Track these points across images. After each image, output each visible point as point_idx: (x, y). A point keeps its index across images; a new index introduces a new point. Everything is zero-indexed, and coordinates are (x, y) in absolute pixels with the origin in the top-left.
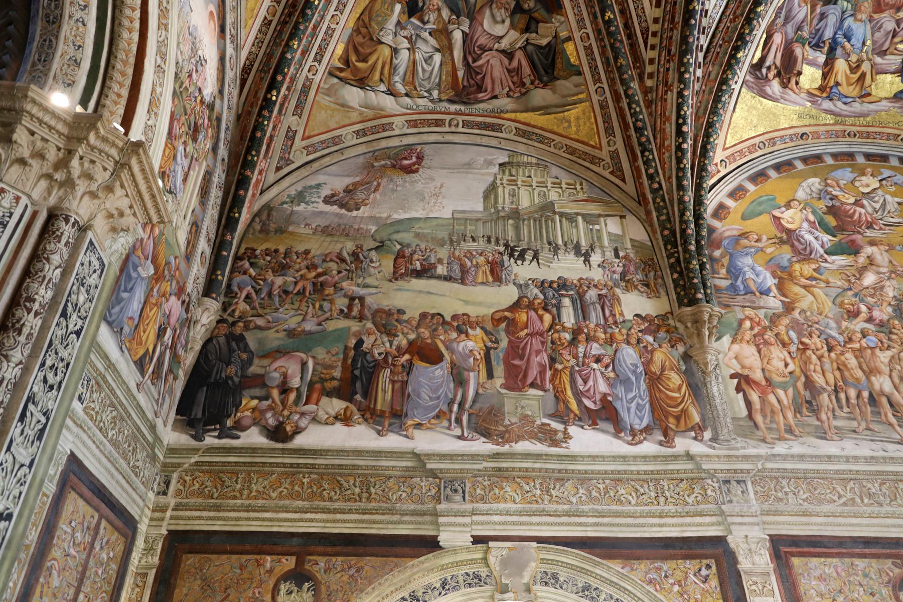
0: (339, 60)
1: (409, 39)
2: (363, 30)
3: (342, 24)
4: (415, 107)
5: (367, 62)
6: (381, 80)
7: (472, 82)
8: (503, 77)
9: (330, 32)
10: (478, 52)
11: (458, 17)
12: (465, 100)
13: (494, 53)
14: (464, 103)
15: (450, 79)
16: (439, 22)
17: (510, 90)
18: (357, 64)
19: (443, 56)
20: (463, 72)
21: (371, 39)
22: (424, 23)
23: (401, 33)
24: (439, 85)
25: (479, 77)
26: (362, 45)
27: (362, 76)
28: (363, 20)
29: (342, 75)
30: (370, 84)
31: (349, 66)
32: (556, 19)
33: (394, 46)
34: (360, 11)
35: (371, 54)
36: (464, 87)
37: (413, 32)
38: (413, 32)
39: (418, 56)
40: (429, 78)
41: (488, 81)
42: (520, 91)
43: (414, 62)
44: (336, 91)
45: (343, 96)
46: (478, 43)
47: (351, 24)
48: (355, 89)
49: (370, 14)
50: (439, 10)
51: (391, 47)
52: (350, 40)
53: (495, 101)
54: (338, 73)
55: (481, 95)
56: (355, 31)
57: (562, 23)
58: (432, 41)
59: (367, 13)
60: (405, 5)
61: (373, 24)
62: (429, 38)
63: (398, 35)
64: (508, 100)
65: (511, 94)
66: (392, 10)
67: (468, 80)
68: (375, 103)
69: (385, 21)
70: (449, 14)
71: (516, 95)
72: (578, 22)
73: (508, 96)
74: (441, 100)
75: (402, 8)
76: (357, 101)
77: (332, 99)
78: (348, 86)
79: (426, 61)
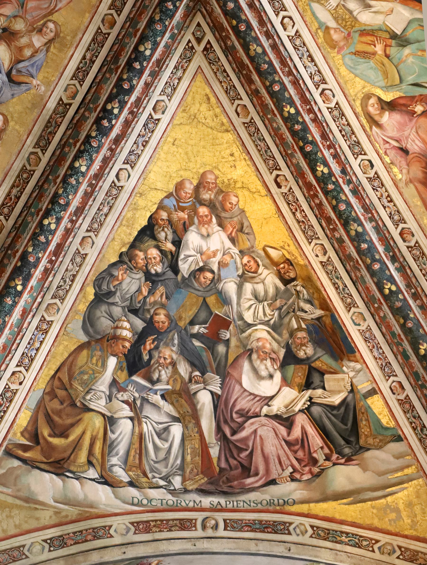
0: (22, 433)
1: (132, 405)
2: (61, 393)
3: (27, 384)
4: (145, 502)
5: (67, 437)
6: (90, 463)
7: (233, 462)
8: (281, 452)
9: (9, 394)
10: (239, 420)
11: (203, 373)
12: (225, 489)
13: (263, 420)
14: (225, 493)
15: (198, 459)
16: (175, 380)
17: (295, 470)
18: (51, 439)
19: (185, 427)
20: (217, 448)
21: (73, 404)
22: (153, 383)
23: (119, 396)
24: (182, 468)
25: (243, 455)
26: (59, 413)
27: (56, 456)
28: (60, 379)
29: (27, 455)
30: (72, 468)
31: (37, 443)
32: (348, 367)
33: (109, 414)
34: (54, 367)
35: (72, 425)
36: (222, 470)
37: (137, 395)
38: (137, 395)
39: (147, 428)
40: (166, 459)
41: (258, 460)
42: (311, 472)
43: (141, 437)
44: (17, 477)
45: (29, 489)
46: (237, 408)
47: (42, 385)
48: (47, 476)
49: (70, 370)
50: (174, 364)
51: (103, 415)
52: (41, 404)
53: (272, 488)
54: (20, 453)
55: (249, 481)
56: (48, 393)
57: (359, 371)
58: (167, 407)
59: (66, 369)
60: (123, 359)
61: (76, 384)
62: (162, 403)
63: (114, 399)
64: (294, 485)
65: (297, 476)
66: (104, 365)
67: (227, 460)
68: (81, 496)
69: (94, 379)
70: (190, 369)
71: (305, 477)
72: (382, 368)
73: (293, 479)
74: (186, 491)
75: (119, 362)
76: (51, 494)
77: (9, 491)
78: (38, 471)
79: (159, 435)
